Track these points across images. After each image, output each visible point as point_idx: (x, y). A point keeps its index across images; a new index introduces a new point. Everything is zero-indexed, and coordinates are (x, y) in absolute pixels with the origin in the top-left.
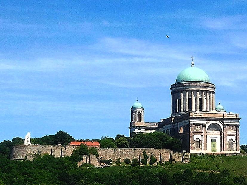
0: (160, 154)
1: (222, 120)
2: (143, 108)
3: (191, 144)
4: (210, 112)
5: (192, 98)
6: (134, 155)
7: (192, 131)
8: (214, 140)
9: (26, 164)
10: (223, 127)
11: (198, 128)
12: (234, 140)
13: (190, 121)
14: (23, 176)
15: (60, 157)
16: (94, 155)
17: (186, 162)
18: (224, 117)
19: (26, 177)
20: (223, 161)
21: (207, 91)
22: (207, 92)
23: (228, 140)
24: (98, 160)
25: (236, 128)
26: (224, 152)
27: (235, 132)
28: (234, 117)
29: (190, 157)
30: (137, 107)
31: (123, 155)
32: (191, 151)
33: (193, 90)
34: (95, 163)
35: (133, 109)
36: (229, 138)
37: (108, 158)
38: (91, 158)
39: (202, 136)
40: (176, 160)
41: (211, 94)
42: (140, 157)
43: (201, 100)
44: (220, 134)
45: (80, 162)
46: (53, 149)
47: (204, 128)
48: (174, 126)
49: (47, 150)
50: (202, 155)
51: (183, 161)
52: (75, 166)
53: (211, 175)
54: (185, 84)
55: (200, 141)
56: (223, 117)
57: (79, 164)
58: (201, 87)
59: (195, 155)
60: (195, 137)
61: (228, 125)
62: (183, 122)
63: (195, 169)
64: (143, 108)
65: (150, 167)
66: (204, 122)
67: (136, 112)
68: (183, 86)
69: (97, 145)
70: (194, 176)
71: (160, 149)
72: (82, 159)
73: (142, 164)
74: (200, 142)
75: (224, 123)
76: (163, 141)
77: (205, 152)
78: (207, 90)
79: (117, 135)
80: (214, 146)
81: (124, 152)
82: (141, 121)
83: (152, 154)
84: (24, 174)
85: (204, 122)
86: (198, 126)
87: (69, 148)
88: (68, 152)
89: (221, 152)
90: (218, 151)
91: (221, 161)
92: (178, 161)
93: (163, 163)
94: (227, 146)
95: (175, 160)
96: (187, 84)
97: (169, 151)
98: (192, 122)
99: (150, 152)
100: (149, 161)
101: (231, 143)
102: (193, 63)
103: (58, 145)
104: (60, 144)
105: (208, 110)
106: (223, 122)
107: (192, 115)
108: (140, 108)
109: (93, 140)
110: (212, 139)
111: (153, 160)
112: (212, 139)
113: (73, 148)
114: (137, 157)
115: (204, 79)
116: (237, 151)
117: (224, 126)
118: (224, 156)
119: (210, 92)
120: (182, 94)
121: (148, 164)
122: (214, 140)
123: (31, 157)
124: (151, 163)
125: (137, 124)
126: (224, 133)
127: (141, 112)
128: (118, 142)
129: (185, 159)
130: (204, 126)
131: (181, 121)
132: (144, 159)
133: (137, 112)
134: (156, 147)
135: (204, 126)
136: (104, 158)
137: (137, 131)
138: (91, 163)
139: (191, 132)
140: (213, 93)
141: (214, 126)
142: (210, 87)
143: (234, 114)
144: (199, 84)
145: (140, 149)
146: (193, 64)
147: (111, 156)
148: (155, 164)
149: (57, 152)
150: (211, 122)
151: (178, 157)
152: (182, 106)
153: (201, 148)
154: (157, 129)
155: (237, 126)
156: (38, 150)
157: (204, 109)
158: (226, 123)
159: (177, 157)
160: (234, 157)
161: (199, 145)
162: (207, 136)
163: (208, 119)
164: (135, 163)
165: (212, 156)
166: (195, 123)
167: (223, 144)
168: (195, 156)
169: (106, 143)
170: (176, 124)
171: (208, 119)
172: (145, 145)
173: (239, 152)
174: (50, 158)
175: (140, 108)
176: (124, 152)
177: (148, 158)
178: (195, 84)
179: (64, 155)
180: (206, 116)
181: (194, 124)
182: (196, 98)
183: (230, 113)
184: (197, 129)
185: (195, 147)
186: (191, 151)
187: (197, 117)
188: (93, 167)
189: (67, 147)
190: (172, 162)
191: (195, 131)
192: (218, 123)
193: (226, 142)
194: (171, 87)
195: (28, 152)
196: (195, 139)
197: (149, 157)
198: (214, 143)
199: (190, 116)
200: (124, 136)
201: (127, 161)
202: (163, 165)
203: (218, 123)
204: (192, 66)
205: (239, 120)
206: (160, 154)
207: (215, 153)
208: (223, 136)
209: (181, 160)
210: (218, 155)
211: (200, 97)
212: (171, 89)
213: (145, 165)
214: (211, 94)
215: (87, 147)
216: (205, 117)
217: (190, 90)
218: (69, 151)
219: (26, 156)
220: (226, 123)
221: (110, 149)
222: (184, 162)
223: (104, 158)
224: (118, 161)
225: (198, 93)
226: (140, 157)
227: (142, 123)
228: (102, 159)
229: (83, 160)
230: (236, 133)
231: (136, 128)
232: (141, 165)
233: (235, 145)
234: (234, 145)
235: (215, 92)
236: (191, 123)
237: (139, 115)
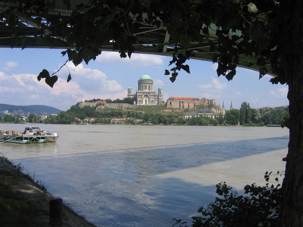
1: (149, 93)
49: (88, 104)
60: (139, 99)
66: (142, 94)
77: (142, 104)
85: (142, 94)
90: (147, 104)
119: (151, 83)
122: (146, 101)
125: (129, 94)
130: (142, 95)
135: (142, 95)
149: (92, 105)
158: (150, 94)
163: (143, 93)
169: (109, 101)
171: (143, 93)
180: (143, 92)
203: (148, 94)
218: (95, 104)
220: (150, 94)
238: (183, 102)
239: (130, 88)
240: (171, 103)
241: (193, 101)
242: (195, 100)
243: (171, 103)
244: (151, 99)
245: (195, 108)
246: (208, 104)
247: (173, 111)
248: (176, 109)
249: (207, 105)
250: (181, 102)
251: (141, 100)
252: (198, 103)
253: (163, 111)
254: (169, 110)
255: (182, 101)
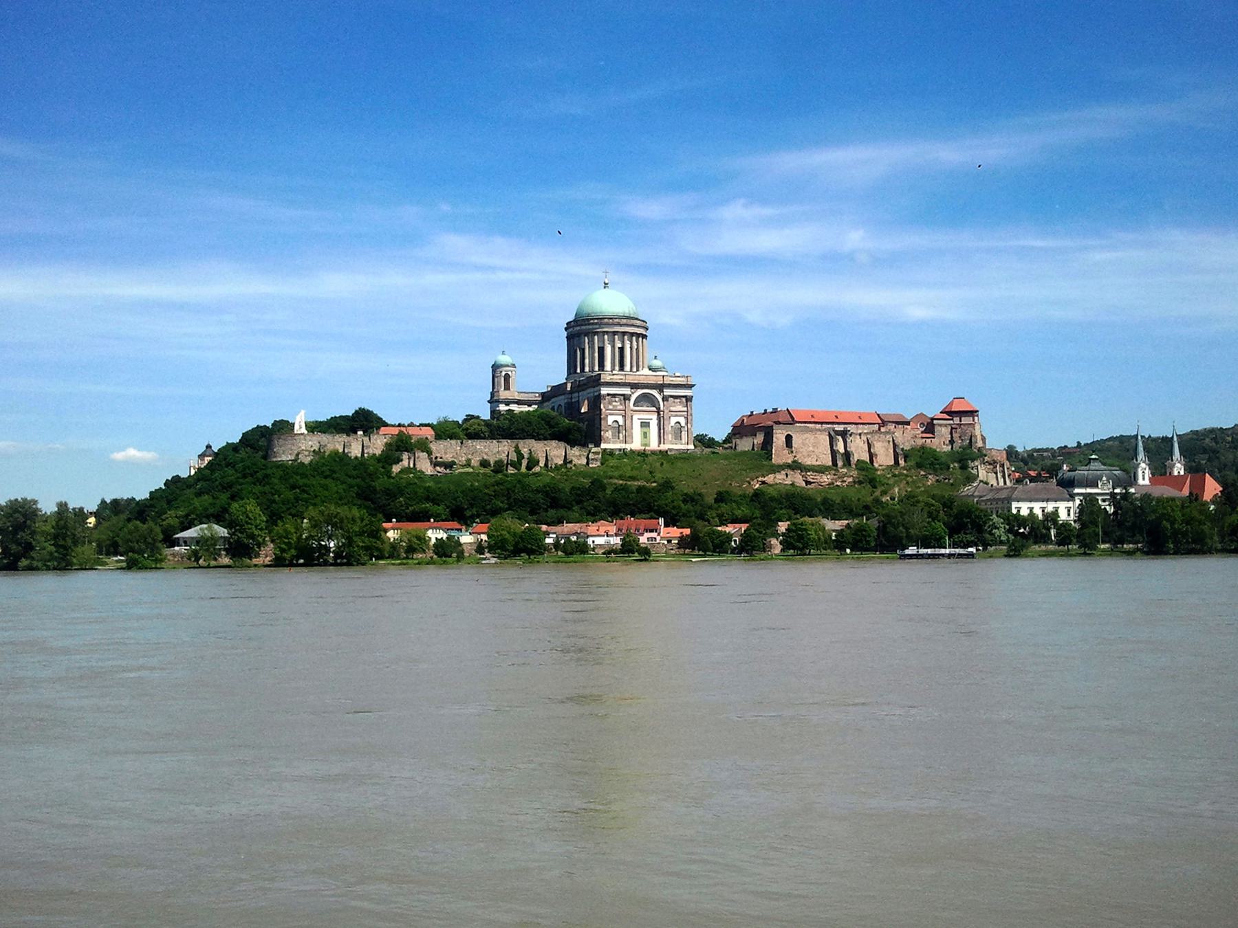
0: (546, 450)
1: (660, 387)
2: (514, 366)
3: (602, 433)
4: (638, 373)
5: (605, 347)
6: (498, 452)
7: (604, 407)
8: (645, 425)
9: (297, 468)
10: (663, 401)
11: (616, 401)
12: (683, 424)
13: (602, 389)
14: (291, 491)
15: (359, 455)
16: (423, 451)
17: (594, 466)
18: (665, 382)
19: (296, 492)
20: (662, 464)
21: (632, 334)
22: (633, 336)
23: (672, 423)
24: (431, 462)
25: (687, 402)
26: (664, 447)
27: (685, 409)
28: (683, 381)
29: (600, 456)
30: (502, 363)
31: (477, 452)
32: (603, 446)
33: (607, 332)
34: (425, 467)
35: (496, 367)
36: (673, 420)
37: (448, 458)
38: (418, 458)
39: (624, 416)
40: (576, 461)
41: (640, 339)
42: (508, 456)
43: (622, 350)
44: (656, 414)
45: (398, 465)
46: (348, 442)
47: (627, 402)
48: (571, 398)
49: (336, 443)
50: (625, 453)
51: (588, 464)
52: (388, 474)
53: (640, 489)
54: (592, 321)
55: (619, 426)
56: (662, 382)
57: (396, 469)
58: (621, 325)
59: (611, 453)
60: (611, 419)
61: (671, 396)
62: (589, 390)
63: (611, 478)
64: (514, 366)
65: (526, 475)
66: (627, 391)
67: (501, 372)
68: (589, 324)
69: (430, 433)
70: (608, 492)
71: (546, 442)
72: (402, 460)
73: (512, 468)
74: (621, 428)
75: (665, 394)
76: (551, 427)
77: (628, 447)
78: (632, 331)
79: (467, 416)
80: (645, 435)
81: (478, 447)
82: (509, 389)
83: (530, 450)
84: (293, 487)
85: (627, 391)
86: (617, 399)
87: (376, 440)
88: (375, 446)
89: (659, 446)
90: (654, 445)
91: (658, 464)
92: (579, 462)
93: (551, 467)
94: (670, 436)
95: (574, 463)
96: (596, 321)
97: (562, 444)
98: (604, 391)
99: (526, 446)
100: (524, 463)
101: (678, 430)
102: (606, 282)
103: (356, 433)
104: (360, 433)
105: (635, 369)
106: (663, 392)
107: (606, 377)
108: (508, 366)
109: (421, 425)
110: (641, 423)
111: (533, 462)
112: (641, 423)
113: (385, 440)
114: (503, 457)
115: (627, 311)
116: (688, 444)
117: (665, 399)
118: (664, 454)
119: (638, 335)
120: (586, 338)
121: (523, 469)
122: (645, 425)
123: (306, 456)
124: (529, 468)
125: (504, 394)
126: (663, 411)
127: (510, 373)
128: (467, 429)
129: (592, 459)
130: (626, 398)
131: (583, 390)
132: (516, 460)
133: (503, 373)
134: (538, 437)
135: (626, 398)
136: (441, 458)
137: (503, 407)
138: (418, 467)
139: (604, 410)
140: (644, 337)
141: (647, 399)
142: (638, 327)
143: (682, 377)
144: (617, 320)
145: (509, 441)
146: (607, 284)
147: (455, 454)
148: (537, 469)
149: (355, 446)
150: (640, 392)
151: (580, 456)
152: (587, 361)
153: (621, 438)
154: (540, 403)
155: (688, 399)
156: (319, 443)
157: (627, 368)
158: (667, 392)
159: (578, 456)
160: (683, 456)
161: (619, 433)
162: (632, 416)
163: (635, 386)
164: (499, 467)
165: (643, 454)
166: (611, 392)
167: (662, 431)
168: (610, 455)
169: (445, 431)
170: (576, 395)
171: (635, 386)
172: (518, 434)
173: (691, 447)
174: (341, 459)
175: (508, 366)
176: (478, 447)
177: (523, 458)
178: (611, 321)
179: (368, 453)
180: (630, 380)
181: (608, 395)
182: (613, 347)
183: (677, 374)
184: (614, 404)
185: (610, 437)
186: (603, 446)
187: (614, 381)
188: (421, 476)
189: (374, 437)
190: (569, 466)
191: (611, 407)
192: (654, 392)
193: (668, 429)
194: (566, 326)
195: (300, 447)
196: (610, 422)
197: (526, 456)
198: (645, 430)
199: (602, 381)
200: (478, 417)
201: (484, 464)
202: (552, 470)
204: (605, 287)
205: (691, 387)
206: (546, 450)
207: (647, 448)
208: (663, 417)
209: (584, 461)
210: (653, 453)
211: (620, 345)
212: (566, 329)
213: (519, 470)
214: (640, 339)
215: (410, 437)
216: (629, 381)
217: (601, 332)
218: (377, 444)
219: (297, 455)
220: (667, 392)
221: (453, 442)
222: (590, 465)
223: (441, 458)
224: (468, 464)
225: (616, 337)
226: (508, 456)
227: (513, 394)
228: (439, 460)
229: (403, 462)
230: (687, 412)
231: (502, 402)
232: (511, 470)
233: (684, 434)
234: (683, 433)
235: (647, 336)
236: (602, 392)
237: (507, 377)
238: (844, 434)
239: (504, 359)
240: (789, 439)
241: (883, 429)
242: (891, 427)
243: (789, 439)
244: (673, 420)
245: (902, 462)
246: (952, 442)
247: (807, 483)
248: (821, 470)
249: (947, 448)
250: (837, 433)
251: (621, 423)
252: (908, 438)
253: (763, 483)
254: (790, 472)
255: (840, 428)
